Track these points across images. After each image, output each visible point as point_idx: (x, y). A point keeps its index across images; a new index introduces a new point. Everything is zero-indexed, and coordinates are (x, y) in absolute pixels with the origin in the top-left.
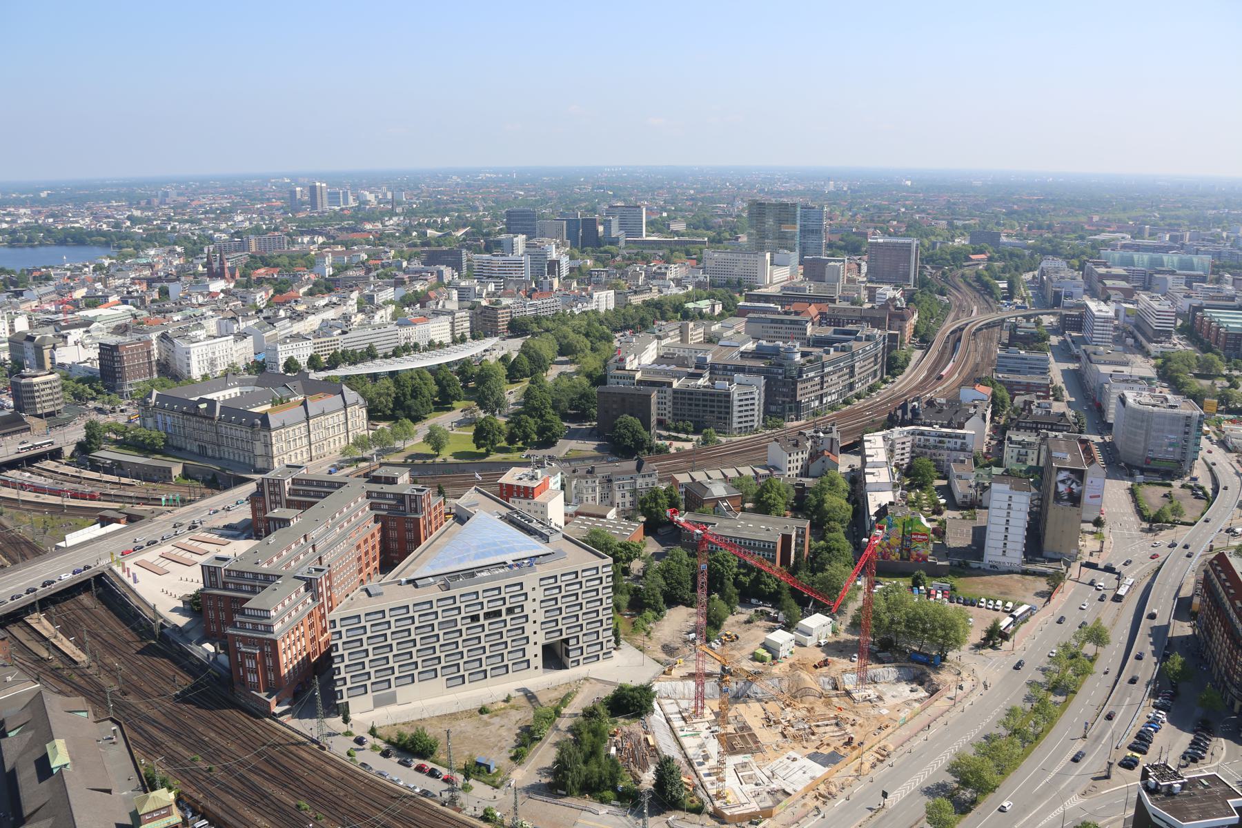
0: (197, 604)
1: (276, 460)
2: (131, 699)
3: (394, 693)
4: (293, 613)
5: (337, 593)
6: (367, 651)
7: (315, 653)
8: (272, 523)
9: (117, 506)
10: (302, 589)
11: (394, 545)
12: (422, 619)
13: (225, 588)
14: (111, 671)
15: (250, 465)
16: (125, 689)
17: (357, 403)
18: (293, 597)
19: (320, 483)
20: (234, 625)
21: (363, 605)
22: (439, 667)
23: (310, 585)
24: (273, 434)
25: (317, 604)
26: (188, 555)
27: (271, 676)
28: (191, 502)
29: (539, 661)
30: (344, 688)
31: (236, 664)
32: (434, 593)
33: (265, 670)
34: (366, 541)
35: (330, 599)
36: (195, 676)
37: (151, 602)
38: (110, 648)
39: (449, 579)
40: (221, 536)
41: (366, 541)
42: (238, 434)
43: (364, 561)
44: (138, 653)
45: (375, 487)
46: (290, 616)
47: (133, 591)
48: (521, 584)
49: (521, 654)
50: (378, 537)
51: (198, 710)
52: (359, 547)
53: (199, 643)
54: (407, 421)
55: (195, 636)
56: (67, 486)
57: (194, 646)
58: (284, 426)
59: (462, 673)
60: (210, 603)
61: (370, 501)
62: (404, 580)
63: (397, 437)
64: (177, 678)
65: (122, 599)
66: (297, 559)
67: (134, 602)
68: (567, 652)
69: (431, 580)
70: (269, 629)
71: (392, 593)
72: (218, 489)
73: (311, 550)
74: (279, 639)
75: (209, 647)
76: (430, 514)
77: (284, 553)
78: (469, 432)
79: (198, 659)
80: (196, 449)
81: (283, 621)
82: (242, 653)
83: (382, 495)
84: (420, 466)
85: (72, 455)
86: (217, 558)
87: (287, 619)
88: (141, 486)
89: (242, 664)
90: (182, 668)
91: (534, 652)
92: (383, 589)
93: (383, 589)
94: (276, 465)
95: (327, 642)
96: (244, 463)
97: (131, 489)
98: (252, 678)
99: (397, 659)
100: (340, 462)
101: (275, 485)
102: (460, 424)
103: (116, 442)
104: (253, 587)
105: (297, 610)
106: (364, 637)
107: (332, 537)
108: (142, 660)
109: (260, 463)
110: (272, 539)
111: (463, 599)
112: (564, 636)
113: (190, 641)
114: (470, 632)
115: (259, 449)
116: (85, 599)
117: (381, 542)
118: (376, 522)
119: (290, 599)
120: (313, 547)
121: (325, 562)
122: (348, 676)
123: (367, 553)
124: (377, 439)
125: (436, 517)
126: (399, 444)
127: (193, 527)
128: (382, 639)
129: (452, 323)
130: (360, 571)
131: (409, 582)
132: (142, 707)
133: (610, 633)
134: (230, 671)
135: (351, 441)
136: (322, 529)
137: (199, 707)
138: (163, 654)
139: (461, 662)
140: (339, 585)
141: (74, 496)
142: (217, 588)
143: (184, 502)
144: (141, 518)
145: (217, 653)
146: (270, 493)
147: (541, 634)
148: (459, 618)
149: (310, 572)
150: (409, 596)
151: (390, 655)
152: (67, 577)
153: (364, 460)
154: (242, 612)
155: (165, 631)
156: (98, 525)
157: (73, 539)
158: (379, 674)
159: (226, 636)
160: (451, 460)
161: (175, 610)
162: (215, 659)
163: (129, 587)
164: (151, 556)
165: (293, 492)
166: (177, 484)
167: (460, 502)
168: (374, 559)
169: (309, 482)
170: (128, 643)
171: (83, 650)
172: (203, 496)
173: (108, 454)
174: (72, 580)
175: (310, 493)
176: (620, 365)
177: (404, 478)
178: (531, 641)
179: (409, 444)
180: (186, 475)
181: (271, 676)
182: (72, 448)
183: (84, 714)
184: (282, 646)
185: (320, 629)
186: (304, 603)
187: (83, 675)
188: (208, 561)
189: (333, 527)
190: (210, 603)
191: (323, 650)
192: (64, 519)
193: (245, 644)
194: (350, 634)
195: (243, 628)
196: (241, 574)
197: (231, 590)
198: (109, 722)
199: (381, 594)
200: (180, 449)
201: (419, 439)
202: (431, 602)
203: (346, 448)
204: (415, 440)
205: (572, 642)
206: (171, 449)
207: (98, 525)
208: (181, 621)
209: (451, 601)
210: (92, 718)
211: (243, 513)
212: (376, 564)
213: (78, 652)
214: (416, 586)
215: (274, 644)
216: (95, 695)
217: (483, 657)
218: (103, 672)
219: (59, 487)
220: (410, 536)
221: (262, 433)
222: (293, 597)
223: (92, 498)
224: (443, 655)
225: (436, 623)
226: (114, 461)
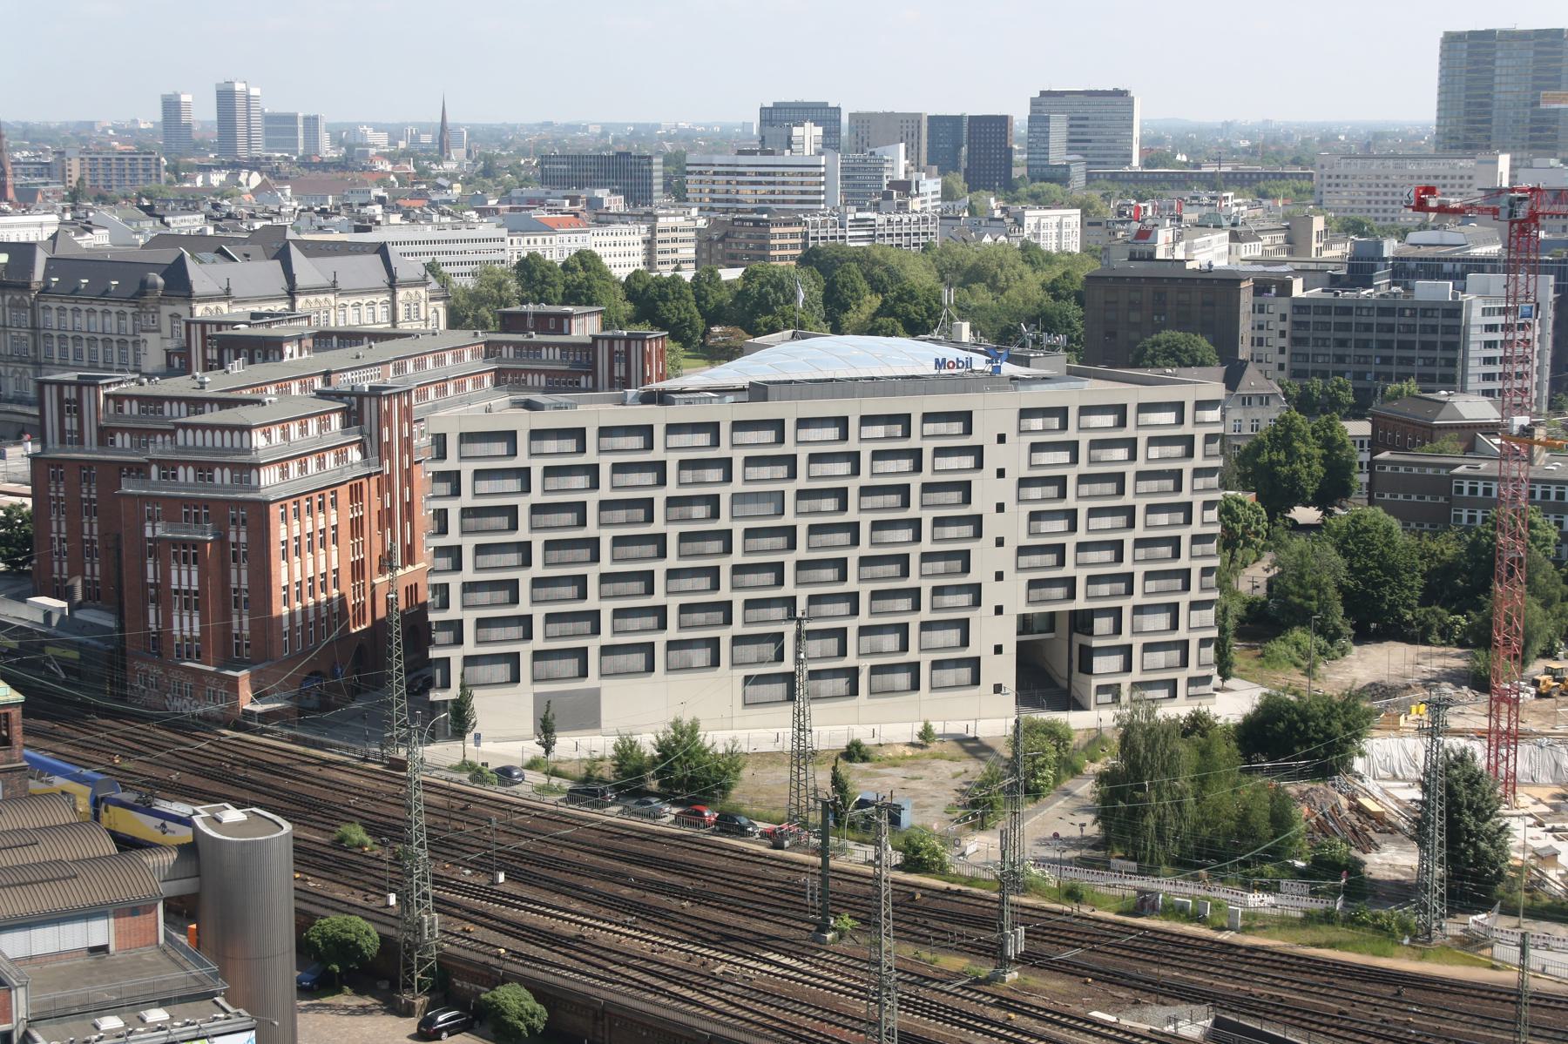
3: (596, 693)
7: (360, 609)
17: (423, 283)
27: (241, 623)
29: (1002, 669)
30: (456, 655)
42: (97, 322)
48: (966, 418)
49: (953, 636)
68: (1087, 654)
70: (247, 469)
91: (994, 636)
98: (186, 625)
112: (1080, 603)
129: (650, 243)
133: (1209, 615)
147: (1017, 584)
176: (1141, 247)
178: (990, 598)
181: (241, 623)
184: (280, 532)
205: (1102, 625)
221: (166, 310)
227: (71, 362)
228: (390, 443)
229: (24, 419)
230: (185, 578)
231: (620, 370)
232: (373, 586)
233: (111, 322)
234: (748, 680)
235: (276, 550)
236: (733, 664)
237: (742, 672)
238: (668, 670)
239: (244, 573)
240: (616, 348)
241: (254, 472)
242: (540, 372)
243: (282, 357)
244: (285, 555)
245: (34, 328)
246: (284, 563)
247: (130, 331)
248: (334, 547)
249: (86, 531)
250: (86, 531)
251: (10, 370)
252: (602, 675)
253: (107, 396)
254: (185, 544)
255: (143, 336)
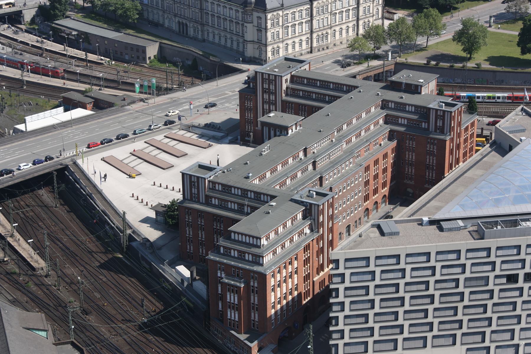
0: (172, 217)
1: (269, 49)
2: (92, 320)
4: (287, 244)
5: (340, 224)
6: (372, 301)
7: (307, 294)
8: (266, 130)
9: (82, 87)
10: (300, 216)
11: (410, 171)
12: (445, 271)
13: (208, 203)
14: (72, 283)
15: (237, 51)
16: (85, 306)
18: (289, 224)
19: (325, 84)
20: (216, 249)
21: (375, 247)
22: (459, 333)
23: (310, 212)
24: (269, 16)
25: (316, 236)
26: (164, 156)
28: (168, 90)
30: (341, 343)
31: (216, 296)
32: (463, 241)
33: (249, 307)
34: (376, 162)
35: (331, 230)
36: (167, 305)
37: (121, 208)
38: (72, 257)
39: (483, 226)
40: (201, 136)
41: (376, 162)
42: (227, 12)
43: (372, 187)
44: (102, 266)
45: (393, 96)
46: (283, 246)
47: (100, 193)
50: (390, 160)
51: (166, 344)
52: (367, 169)
53: (173, 264)
54: (434, 12)
55: (169, 256)
56: (27, 58)
57: (167, 268)
58: (282, 7)
59: (487, 344)
60: (189, 219)
61: (384, 113)
62: (426, 219)
63: (419, 30)
64: (146, 302)
65: (86, 200)
66: (294, 177)
67: (100, 205)
69: (461, 223)
70: (257, 260)
71: (410, 233)
72: (202, 80)
73: (310, 167)
74: (269, 273)
75: (184, 270)
76: (459, 135)
77: (279, 168)
78: (514, 32)
79: (171, 284)
80: (175, 27)
81: (274, 252)
82: (224, 284)
83: (401, 107)
84: (449, 71)
85: (33, 21)
86: (201, 167)
87: (279, 250)
88: (110, 66)
89: (223, 298)
90: (152, 292)
92: (399, 228)
93: (399, 228)
94: (269, 54)
95: (322, 282)
96: (231, 49)
97: (99, 68)
98: (232, 315)
99: (408, 316)
100: (347, 57)
101: (270, 82)
102: (501, 19)
103: (82, 9)
104: (241, 205)
105: (291, 240)
106: (372, 285)
107: (337, 154)
108: (105, 276)
109: (250, 51)
110: (266, 148)
111: (500, 253)
113: (162, 261)
114: (503, 294)
115: (250, 33)
116: (44, 194)
117: (395, 165)
118: (390, 139)
119: (285, 226)
120: (314, 164)
121: (326, 183)
122: (347, 329)
123: (376, 177)
124: (394, 31)
125: (466, 140)
126: (421, 41)
127: (169, 123)
128: (393, 289)
130: (366, 198)
131: (432, 222)
132: (103, 330)
134: (207, 303)
135: (361, 31)
136: (325, 143)
137: (167, 340)
138: (132, 273)
139: (488, 331)
140: (341, 213)
141: (36, 71)
142: (198, 202)
143: (160, 91)
144: (110, 105)
145: (192, 279)
146: (264, 91)
148: (492, 275)
149: (310, 196)
150: (432, 241)
151: (401, 310)
152: (26, 167)
153: (376, 57)
154: (228, 236)
155: (134, 244)
156: (61, 109)
157: (34, 122)
158: (383, 332)
159: (206, 261)
160: (486, 66)
161: (146, 220)
162: (190, 285)
163: (95, 186)
164: (121, 152)
165: (291, 92)
166: (151, 67)
167: (503, 124)
168: (384, 185)
169: (312, 82)
170: (90, 252)
171: (42, 256)
172: (181, 86)
173: (73, 23)
174: (30, 172)
175: (313, 95)
177: (430, 86)
179: (434, 41)
180: (162, 57)
181: (255, 316)
182: (33, 12)
183: (44, 334)
184: (271, 282)
185: (316, 265)
186: (301, 233)
187: (41, 285)
188: (190, 168)
189: (339, 140)
190: (189, 219)
191: (317, 290)
192: (23, 97)
193: (229, 275)
194: (354, 278)
195: (227, 254)
196: (227, 188)
197: (214, 206)
198: (69, 346)
199: (397, 234)
200: (157, 25)
201: (447, 35)
202: (458, 252)
203: (355, 40)
204: (443, 37)
206: (145, 24)
207: (61, 109)
208: (152, 234)
209: (484, 254)
210: (52, 339)
211: (229, 111)
212: (385, 191)
213: (37, 257)
214: (441, 229)
215: (262, 278)
216: (55, 313)
217: (517, 328)
218: (63, 284)
219: (18, 58)
220: (431, 161)
221: (255, 14)
222: (289, 224)
223: (55, 75)
224: (465, 319)
225: (462, 278)
226: (81, 33)
227: (216, 26)
228: (323, 222)
229: (196, 54)
230: (232, 298)
231: (439, 123)
232: (313, 282)
233: (233, 13)
234: (468, 350)
235: (269, 288)
236: (462, 344)
237: (466, 347)
238: (433, 347)
239: (256, 298)
240: (439, 113)
241: (261, 258)
242: (404, 118)
243: (288, 134)
244: (273, 290)
245: (201, 9)
246: (273, 293)
247: (240, 19)
248: (296, 276)
249: (200, 236)
250: (200, 236)
251: (191, 25)
252: (404, 349)
253: (209, 181)
254: (233, 286)
255: (245, 24)
